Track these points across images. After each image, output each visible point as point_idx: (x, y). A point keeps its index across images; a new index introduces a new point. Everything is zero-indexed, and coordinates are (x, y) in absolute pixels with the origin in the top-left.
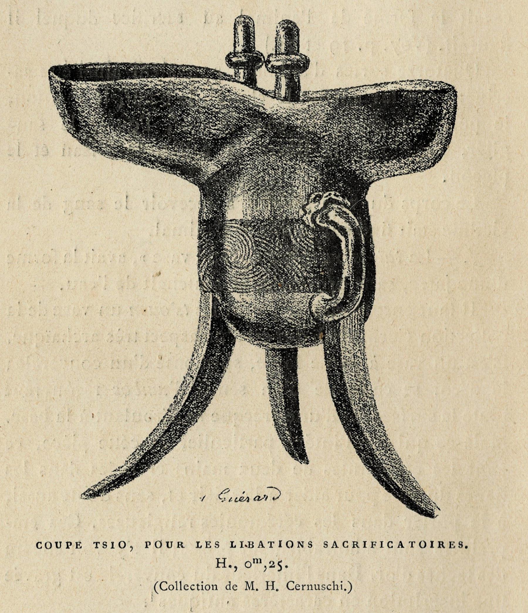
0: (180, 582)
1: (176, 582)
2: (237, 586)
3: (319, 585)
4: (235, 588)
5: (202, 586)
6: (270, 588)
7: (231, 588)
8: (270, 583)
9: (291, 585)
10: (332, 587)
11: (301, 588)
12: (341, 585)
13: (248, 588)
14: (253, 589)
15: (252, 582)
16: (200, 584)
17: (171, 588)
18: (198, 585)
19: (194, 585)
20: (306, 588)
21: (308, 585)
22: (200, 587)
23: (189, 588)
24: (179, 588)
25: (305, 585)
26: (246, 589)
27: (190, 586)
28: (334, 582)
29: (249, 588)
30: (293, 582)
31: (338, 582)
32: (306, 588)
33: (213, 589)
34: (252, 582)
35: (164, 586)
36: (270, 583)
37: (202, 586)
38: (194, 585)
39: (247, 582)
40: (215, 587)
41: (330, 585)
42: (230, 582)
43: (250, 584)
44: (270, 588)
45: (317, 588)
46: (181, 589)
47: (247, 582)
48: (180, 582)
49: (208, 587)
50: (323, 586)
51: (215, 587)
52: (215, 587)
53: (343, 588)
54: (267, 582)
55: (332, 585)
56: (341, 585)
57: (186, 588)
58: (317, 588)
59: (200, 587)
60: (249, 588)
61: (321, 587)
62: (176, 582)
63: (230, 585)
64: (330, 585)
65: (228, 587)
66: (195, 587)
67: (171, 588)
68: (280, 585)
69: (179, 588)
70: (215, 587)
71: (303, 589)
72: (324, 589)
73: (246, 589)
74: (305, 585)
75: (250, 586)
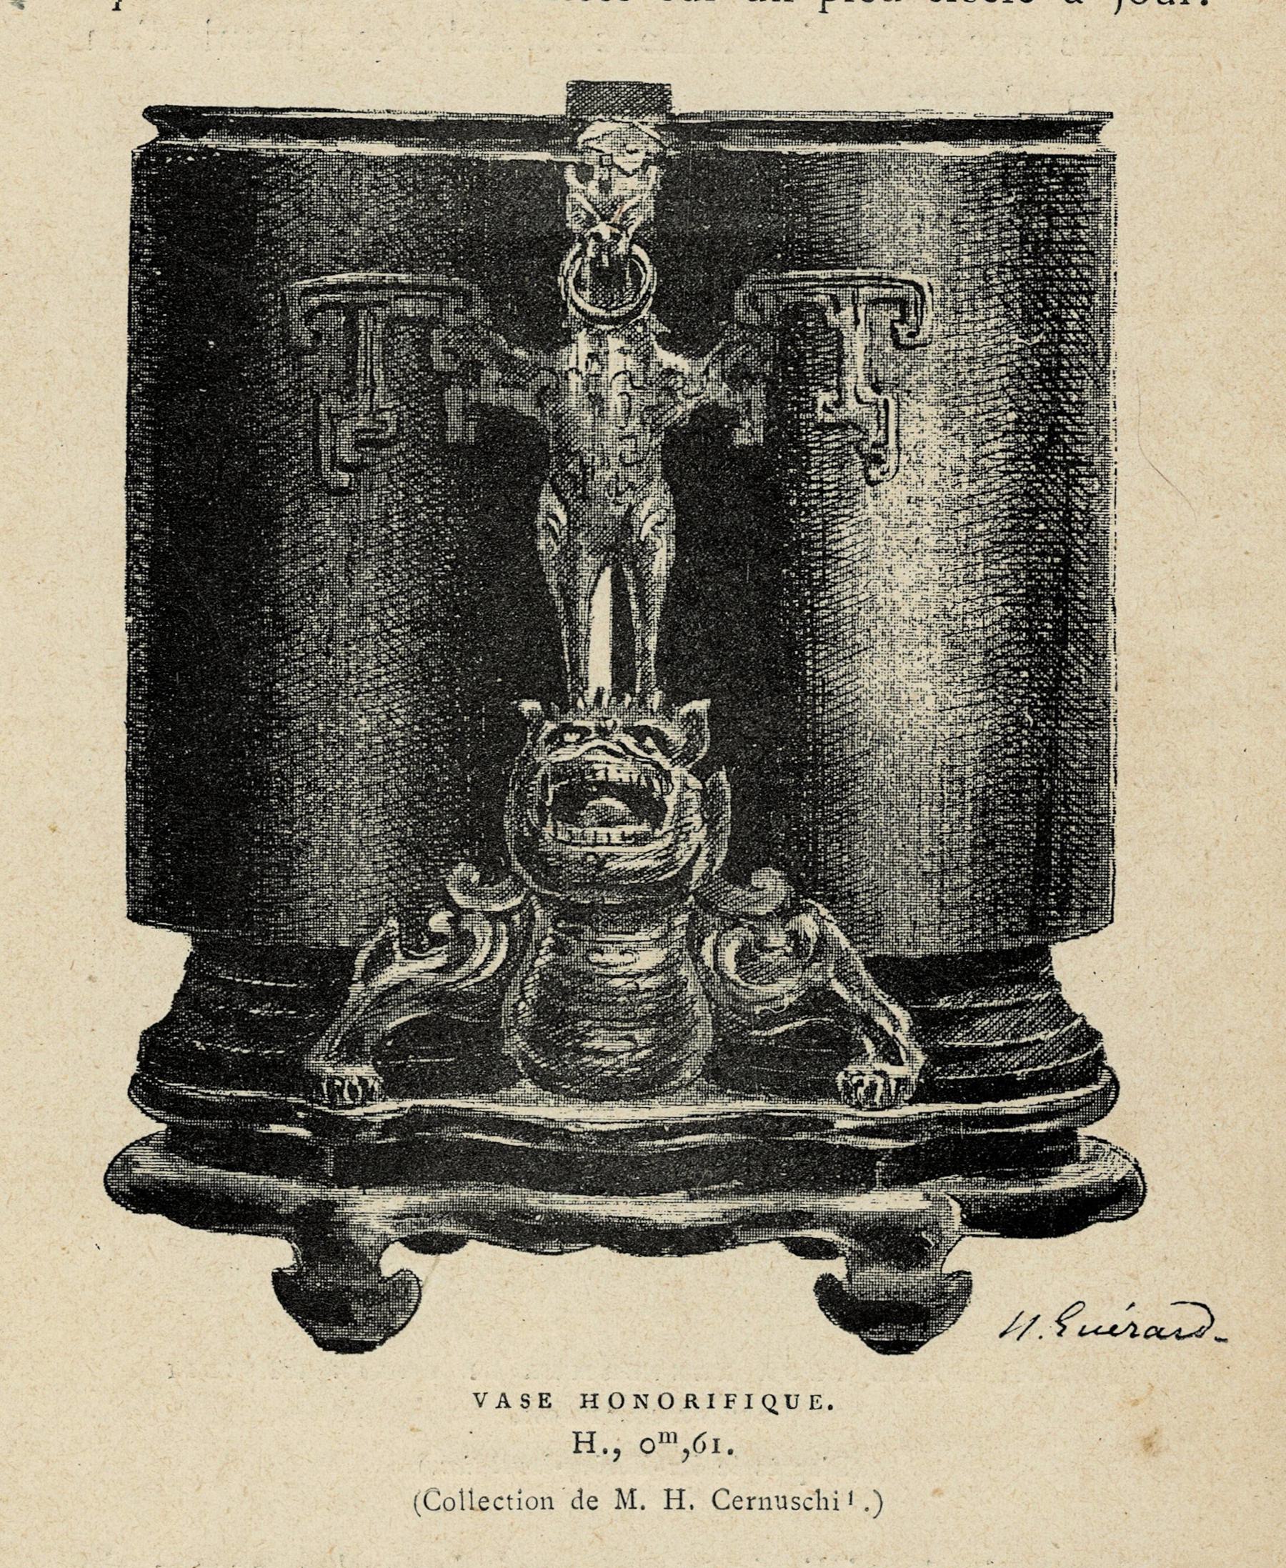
4: (593, 1504)
7: (585, 1505)
9: (723, 1500)
10: (814, 1504)
11: (745, 1503)
14: (633, 1507)
16: (515, 1496)
17: (449, 1504)
22: (515, 1504)
23: (490, 1505)
24: (467, 1504)
27: (492, 1502)
28: (818, 1491)
30: (728, 1492)
32: (756, 1504)
35: (434, 1501)
38: (501, 1498)
40: (546, 1503)
45: (782, 1505)
49: (532, 1503)
51: (546, 1503)
52: (547, 1503)
54: (668, 1491)
55: (815, 1498)
57: (484, 1505)
59: (515, 1504)
61: (790, 1505)
65: (577, 1504)
67: (449, 1504)
69: (467, 1504)
70: (547, 1503)
71: (750, 1508)
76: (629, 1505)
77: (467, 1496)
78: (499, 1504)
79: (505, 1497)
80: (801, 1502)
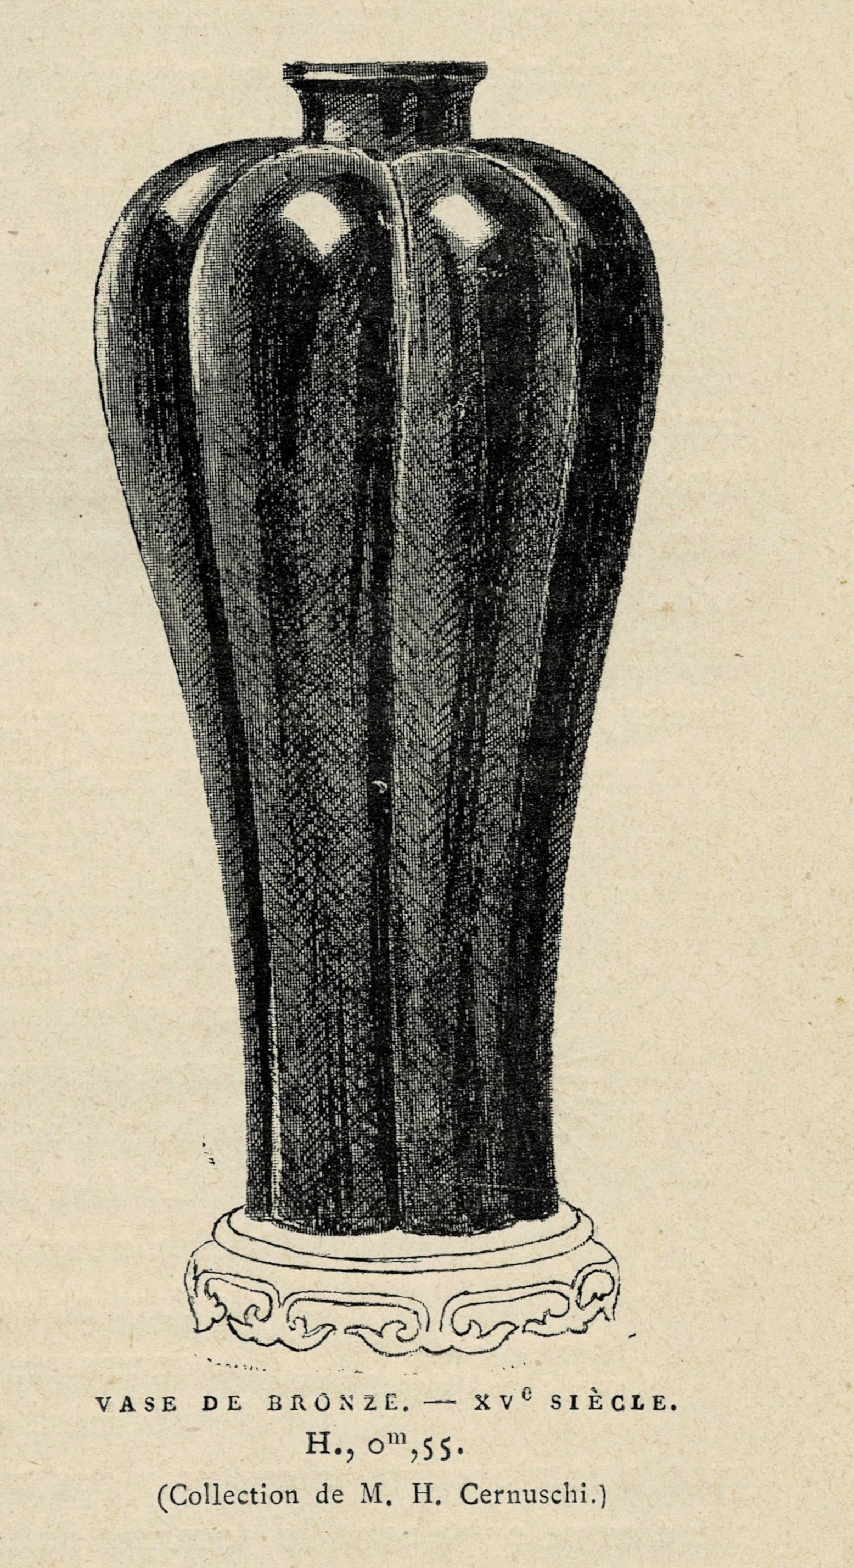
8: (422, 1488)
9: (471, 1494)
12: (583, 1492)
13: (367, 1499)
14: (378, 1501)
16: (259, 1489)
18: (253, 1492)
19: (245, 1492)
21: (509, 1492)
22: (258, 1498)
23: (235, 1499)
24: (212, 1499)
25: (502, 1492)
26: (364, 1502)
29: (370, 1498)
36: (422, 1488)
37: (263, 1493)
41: (559, 1492)
43: (371, 1488)
45: (530, 1498)
46: (217, 1503)
47: (365, 1485)
50: (544, 1493)
55: (563, 1489)
56: (583, 1492)
58: (530, 1498)
61: (538, 1498)
63: (325, 1492)
64: (559, 1492)
66: (248, 1497)
67: (195, 1498)
71: (497, 1502)
72: (544, 1500)
73: (364, 1502)
74: (502, 1492)
75: (373, 1494)
76: (374, 1499)
77: (212, 1490)
78: (243, 1497)
79: (249, 1491)
80: (549, 1496)
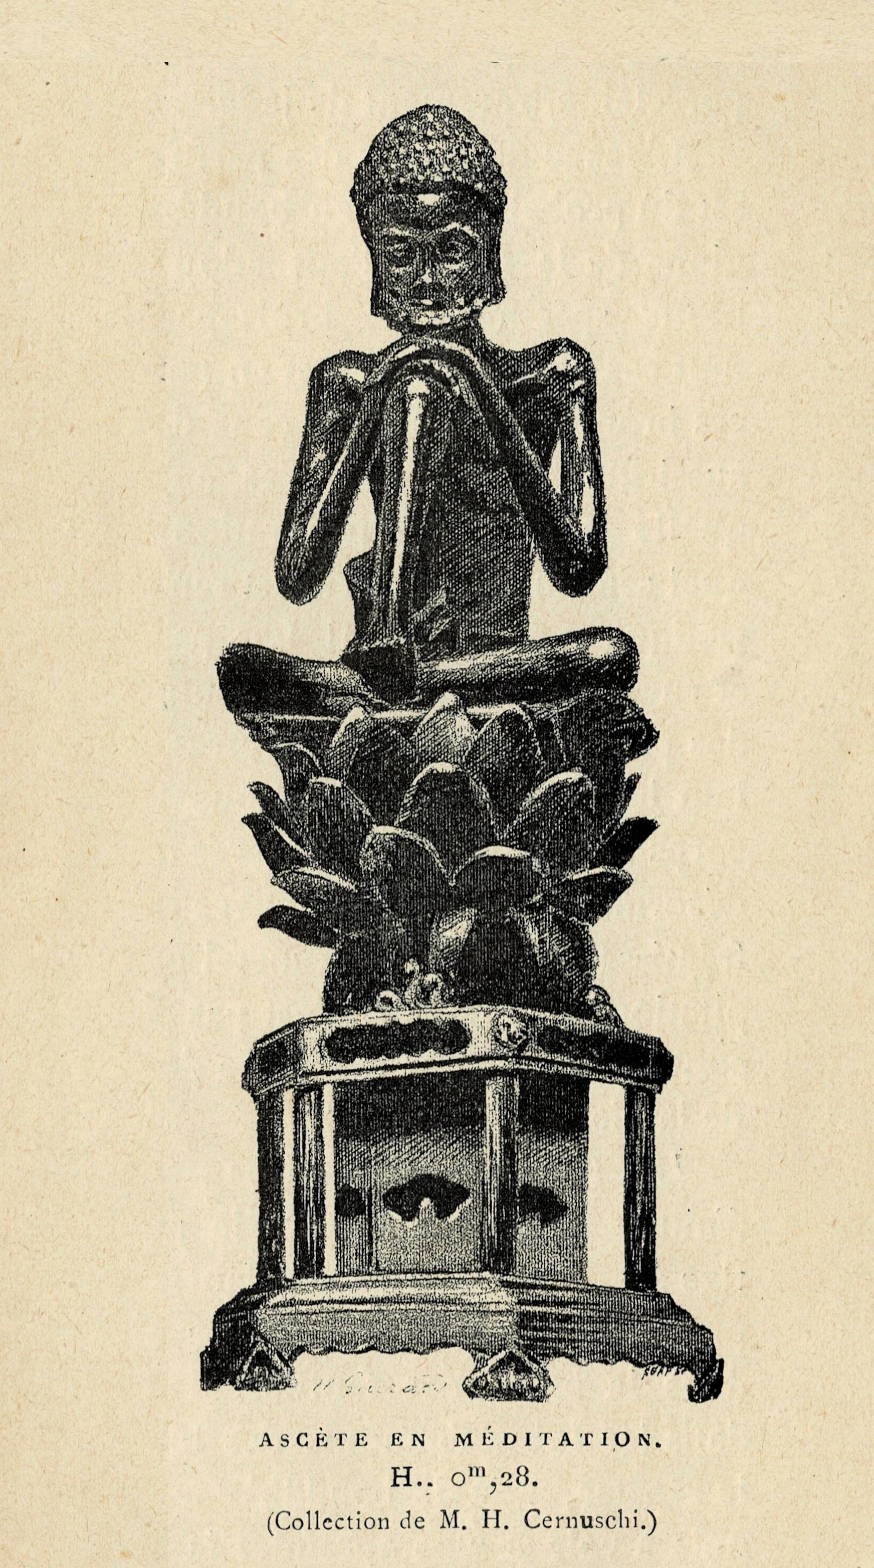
0: (317, 1513)
1: (309, 1513)
2: (423, 1520)
3: (590, 1518)
5: (358, 1520)
6: (492, 1523)
9: (533, 1519)
11: (554, 1523)
12: (635, 1518)
13: (446, 1524)
15: (455, 1513)
16: (355, 1517)
17: (297, 1524)
19: (342, 1519)
20: (563, 1523)
21: (568, 1518)
22: (354, 1524)
23: (332, 1524)
24: (313, 1526)
28: (620, 1511)
29: (449, 1524)
31: (628, 1513)
33: (381, 1528)
34: (455, 1513)
35: (284, 1521)
37: (358, 1520)
38: (342, 1519)
39: (445, 1513)
42: (409, 1512)
44: (492, 1523)
45: (587, 1523)
46: (317, 1528)
47: (445, 1513)
48: (317, 1513)
49: (370, 1523)
50: (599, 1520)
53: (639, 1525)
55: (617, 1516)
56: (635, 1518)
58: (587, 1523)
59: (354, 1524)
60: (449, 1524)
61: (594, 1523)
62: (309, 1513)
67: (297, 1524)
68: (512, 1517)
69: (313, 1526)
75: (450, 1519)
76: (453, 1524)
78: (340, 1524)
